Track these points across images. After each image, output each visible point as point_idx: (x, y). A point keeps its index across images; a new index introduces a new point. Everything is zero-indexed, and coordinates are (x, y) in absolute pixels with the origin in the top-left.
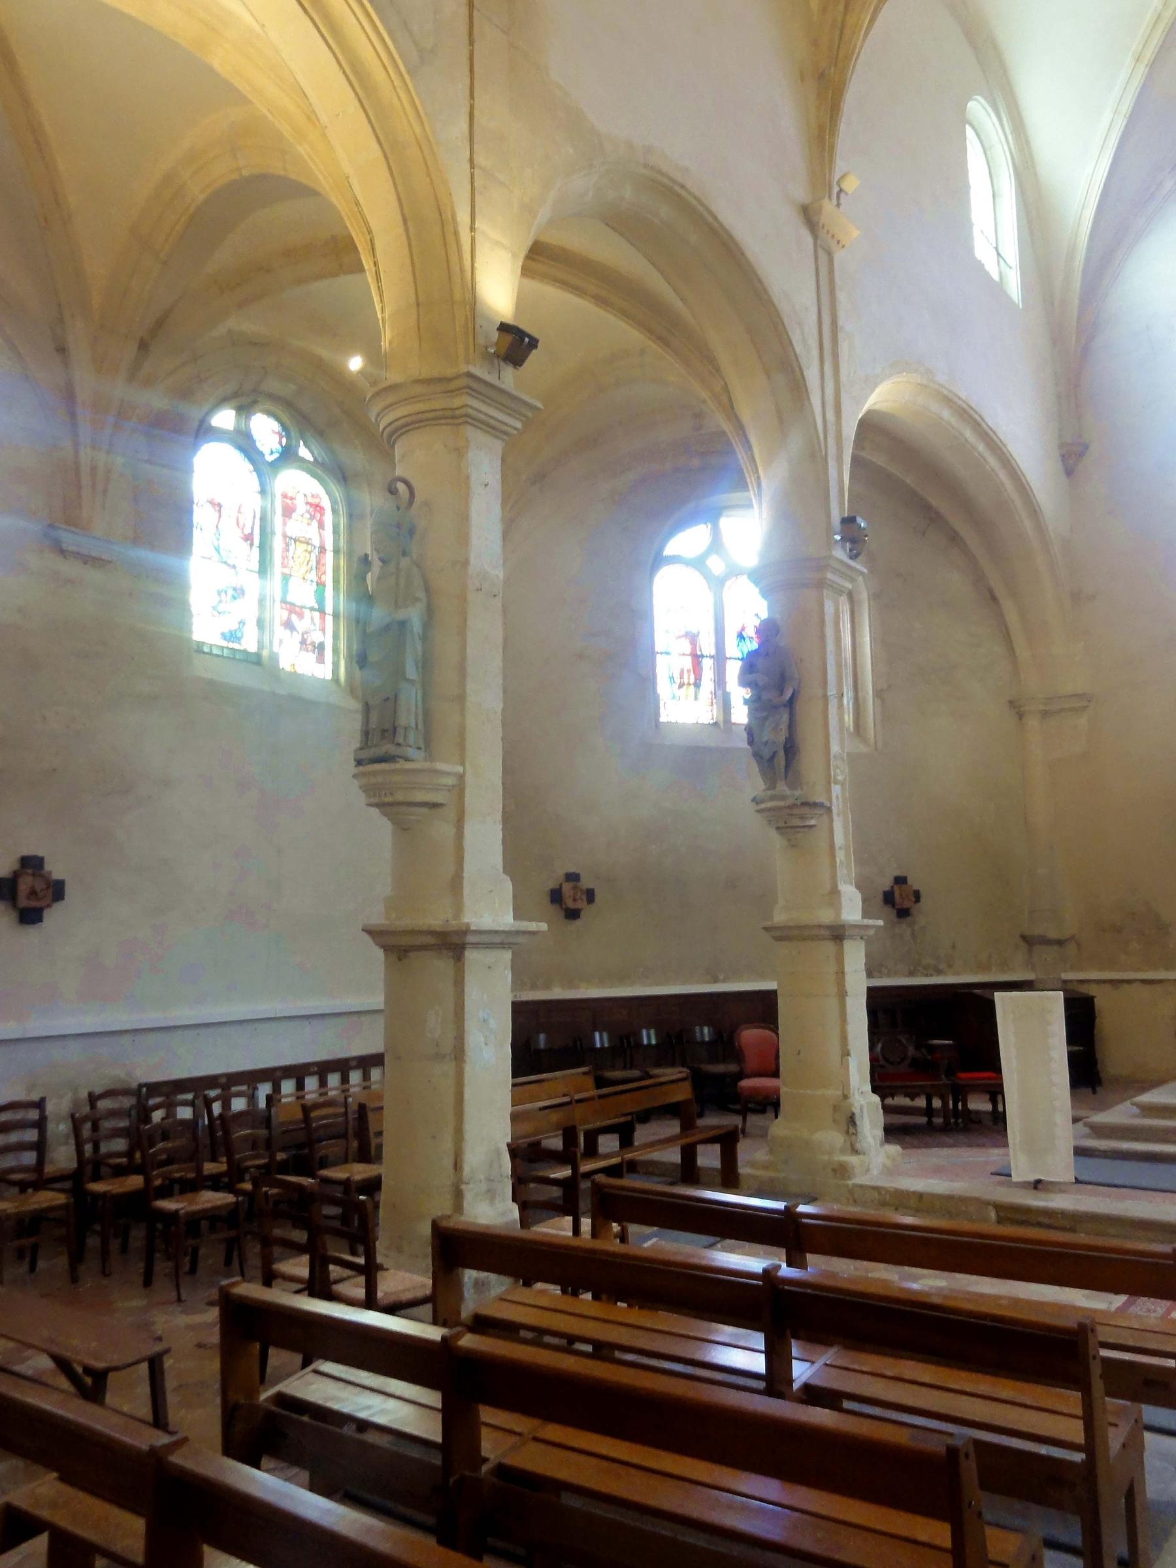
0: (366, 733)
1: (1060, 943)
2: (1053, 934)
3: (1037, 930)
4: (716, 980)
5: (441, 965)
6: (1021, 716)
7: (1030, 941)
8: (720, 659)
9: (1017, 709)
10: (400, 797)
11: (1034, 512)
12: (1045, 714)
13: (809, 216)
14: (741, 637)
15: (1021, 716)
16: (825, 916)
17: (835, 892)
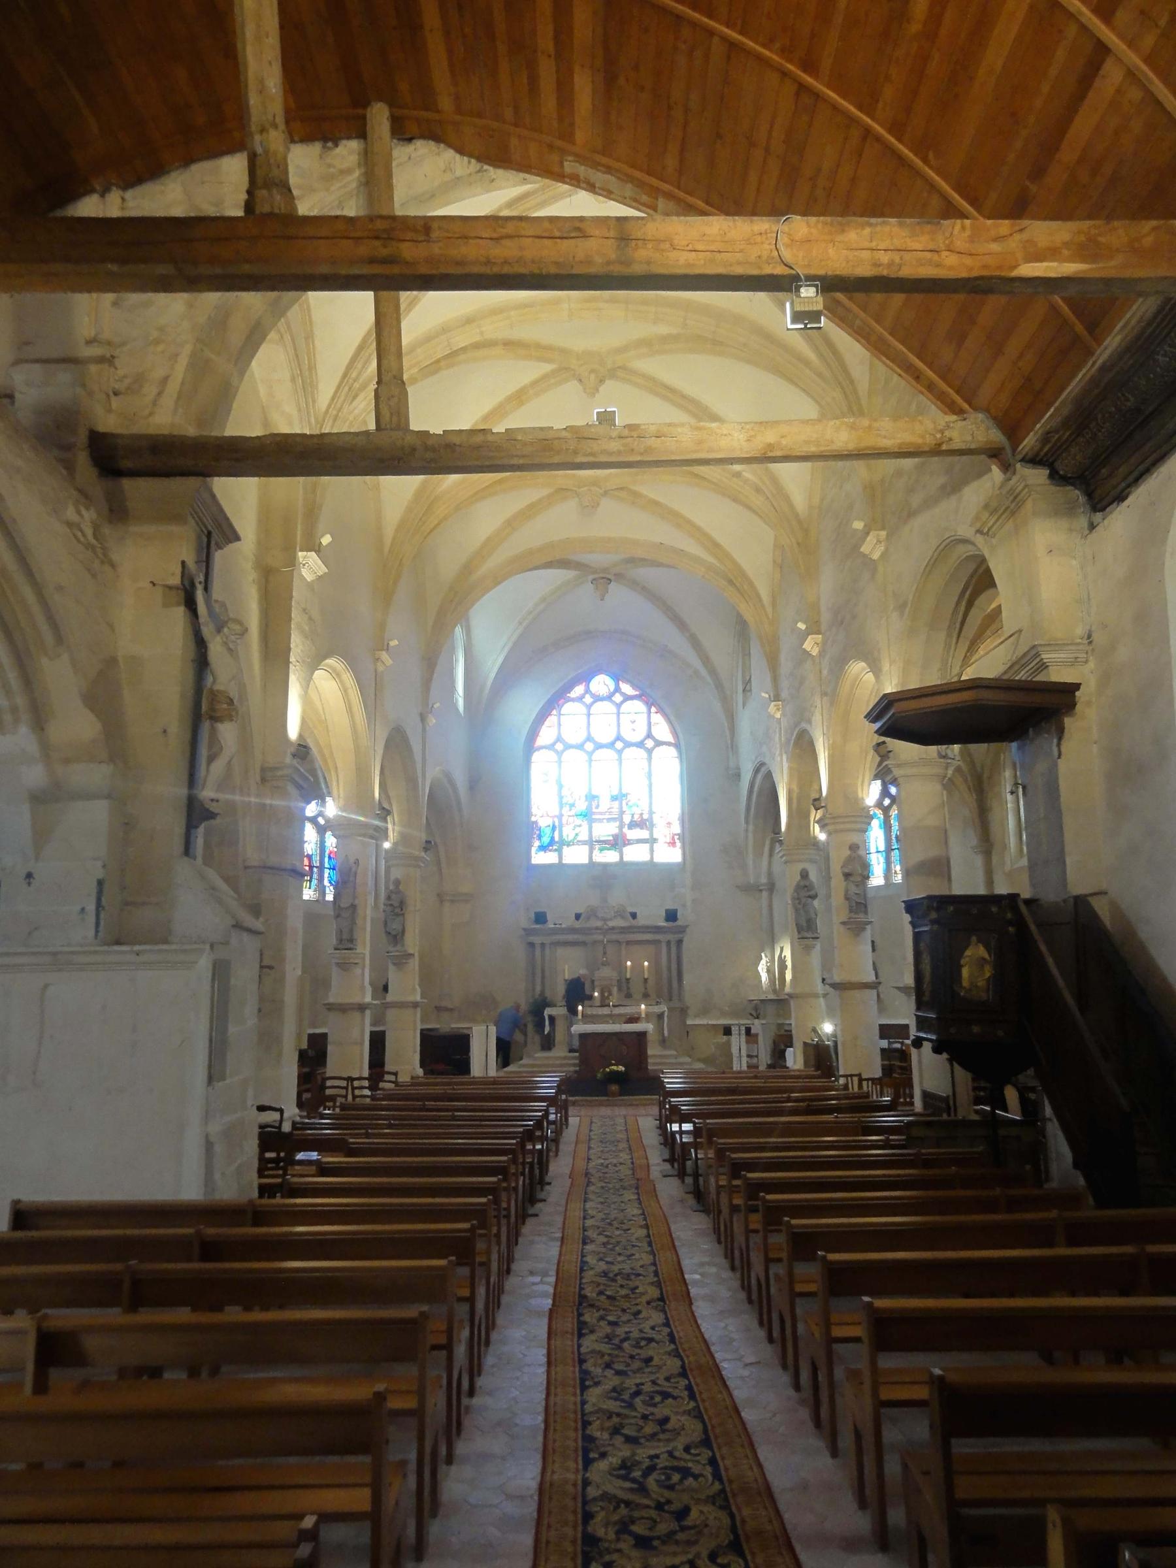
0: (341, 941)
1: (451, 1010)
2: (450, 1006)
3: (444, 1004)
4: (315, 1027)
5: (357, 1015)
6: (442, 901)
7: (438, 1009)
8: (321, 868)
9: (441, 898)
10: (351, 961)
11: (460, 810)
12: (452, 901)
13: (423, 718)
14: (330, 858)
15: (442, 901)
16: (411, 998)
17: (414, 989)
